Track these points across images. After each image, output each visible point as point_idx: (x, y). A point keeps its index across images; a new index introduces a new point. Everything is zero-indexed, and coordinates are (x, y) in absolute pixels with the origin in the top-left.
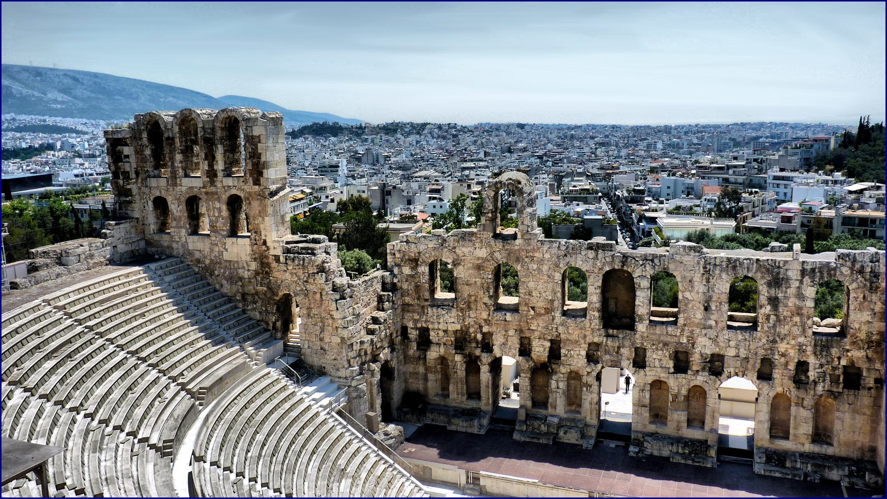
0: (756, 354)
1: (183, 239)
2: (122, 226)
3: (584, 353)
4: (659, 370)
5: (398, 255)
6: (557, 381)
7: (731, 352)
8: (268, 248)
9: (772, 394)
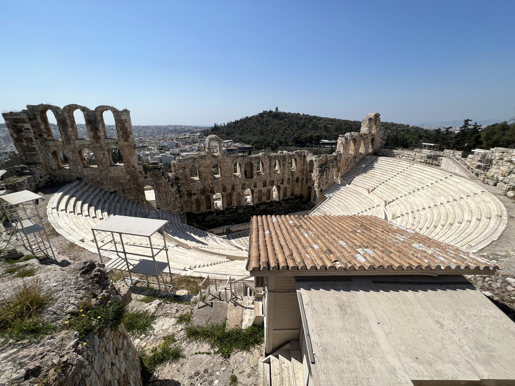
1: (80, 171)
2: (38, 167)
5: (177, 166)
8: (136, 169)
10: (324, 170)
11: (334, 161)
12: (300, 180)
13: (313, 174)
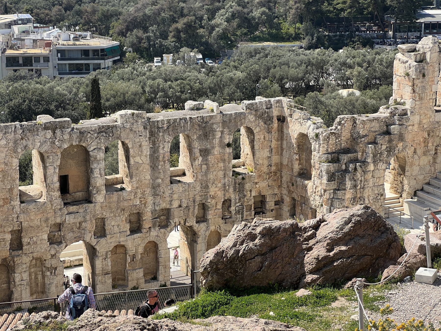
0: (194, 201)
3: (46, 237)
4: (118, 235)
6: (20, 273)
7: (176, 204)
9: (208, 233)
10: (346, 171)
11: (380, 140)
12: (270, 204)
13: (309, 184)
